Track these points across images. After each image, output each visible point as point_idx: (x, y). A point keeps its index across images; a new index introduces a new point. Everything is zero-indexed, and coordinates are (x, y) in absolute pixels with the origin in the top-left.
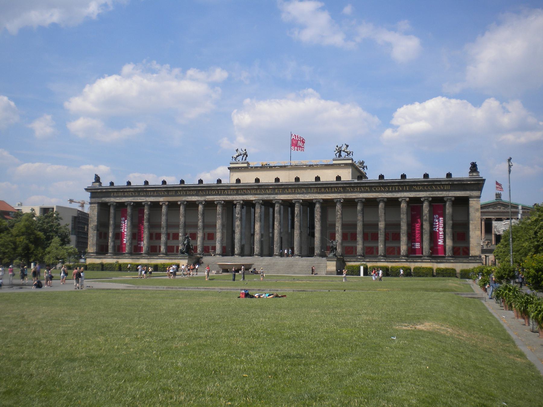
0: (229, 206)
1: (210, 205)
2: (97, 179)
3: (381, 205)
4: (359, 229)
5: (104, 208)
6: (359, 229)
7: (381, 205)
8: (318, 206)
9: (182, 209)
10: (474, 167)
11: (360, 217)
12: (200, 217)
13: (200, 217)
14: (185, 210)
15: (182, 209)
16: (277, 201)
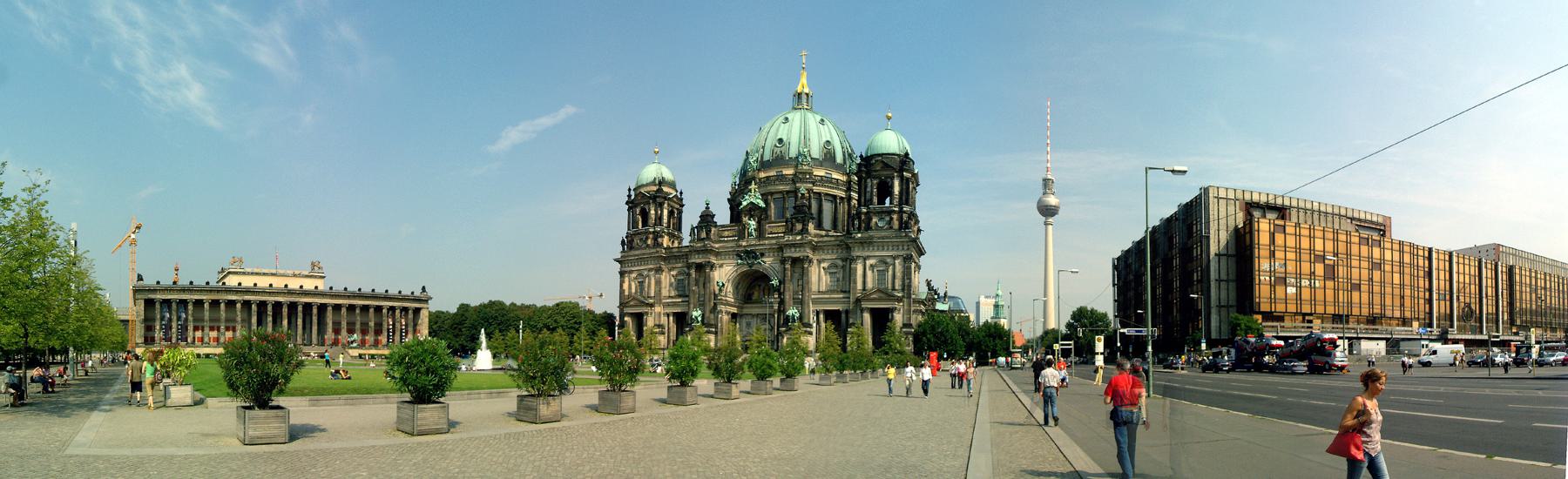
0: (262, 305)
1: (247, 304)
2: (140, 278)
3: (372, 310)
4: (358, 326)
5: (149, 304)
6: (358, 326)
7: (372, 310)
8: (330, 308)
9: (222, 305)
10: (424, 288)
11: (358, 318)
12: (239, 313)
13: (239, 313)
14: (226, 307)
15: (222, 305)
16: (301, 304)
